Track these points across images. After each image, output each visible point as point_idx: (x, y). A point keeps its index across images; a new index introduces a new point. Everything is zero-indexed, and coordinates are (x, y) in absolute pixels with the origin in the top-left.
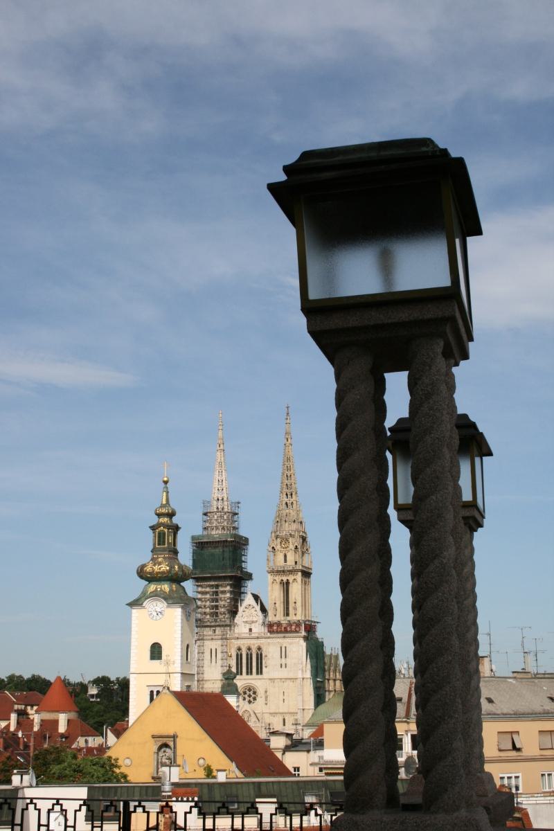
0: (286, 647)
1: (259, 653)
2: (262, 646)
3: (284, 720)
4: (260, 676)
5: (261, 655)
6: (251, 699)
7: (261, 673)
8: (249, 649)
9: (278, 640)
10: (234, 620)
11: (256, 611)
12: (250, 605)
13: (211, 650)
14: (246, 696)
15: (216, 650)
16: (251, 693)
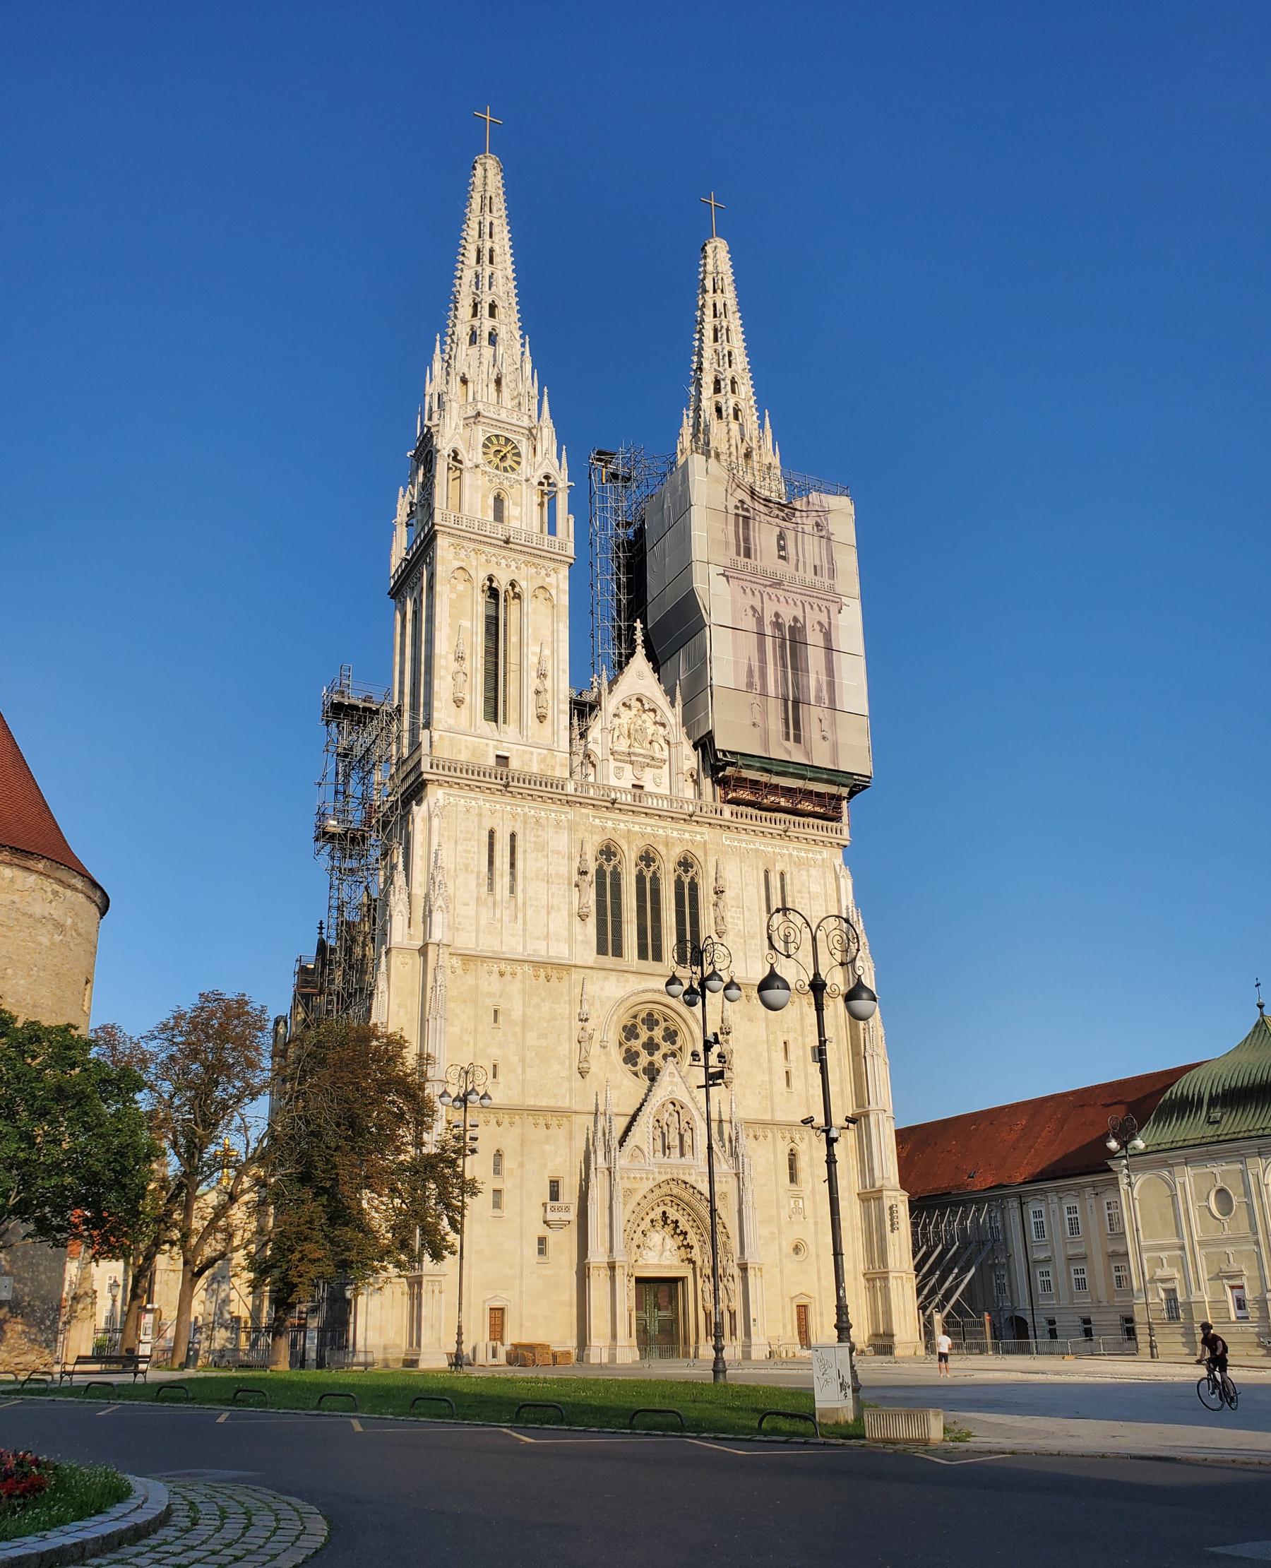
0: (782, 874)
1: (687, 881)
2: (699, 854)
3: (793, 1156)
5: (694, 887)
8: (647, 858)
9: (759, 844)
10: (583, 736)
13: (492, 834)
15: (513, 836)
16: (658, 1033)
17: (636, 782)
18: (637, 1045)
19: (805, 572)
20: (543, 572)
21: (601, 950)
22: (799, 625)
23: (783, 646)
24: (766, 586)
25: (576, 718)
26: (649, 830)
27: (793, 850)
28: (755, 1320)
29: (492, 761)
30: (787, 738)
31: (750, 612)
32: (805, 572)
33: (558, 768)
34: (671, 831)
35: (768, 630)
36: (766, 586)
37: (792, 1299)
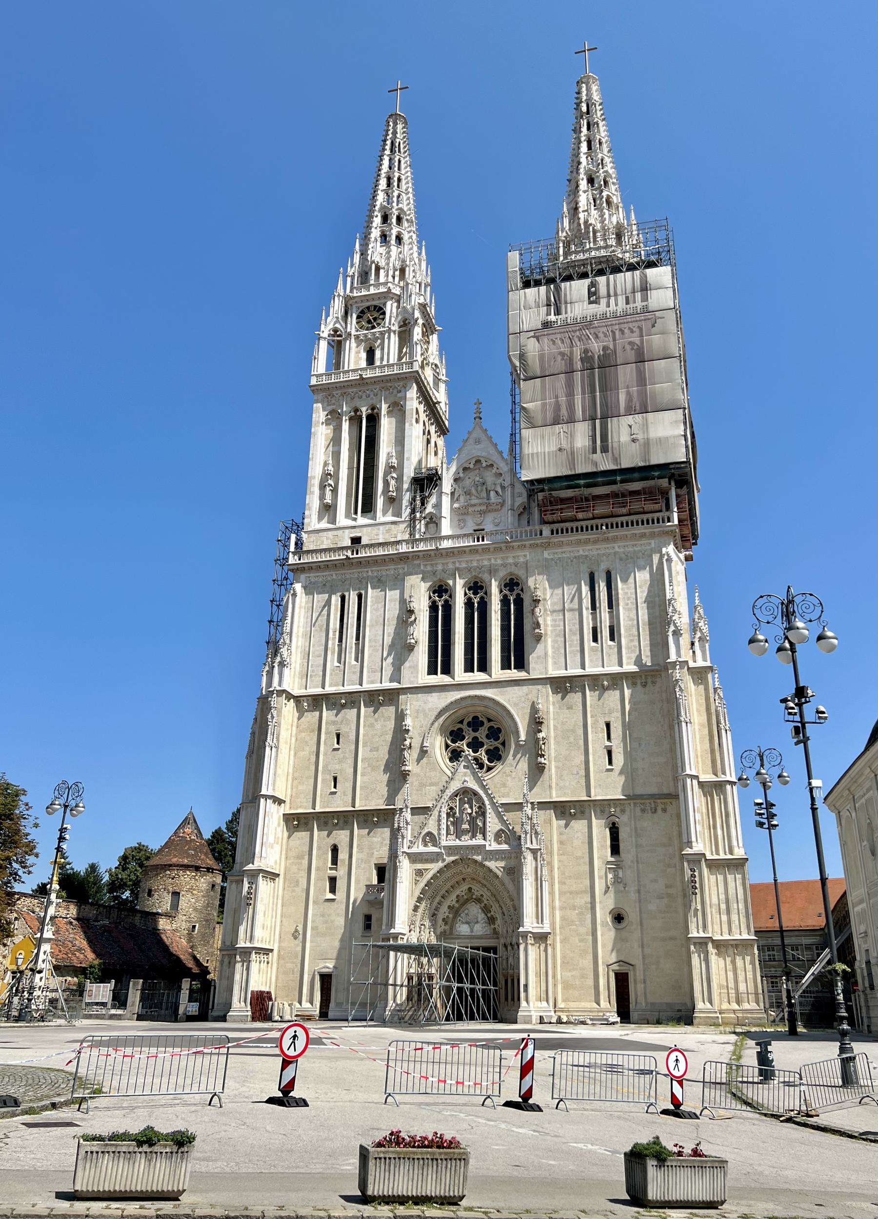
4: (514, 674)
5: (519, 602)
6: (482, 754)
7: (521, 665)
9: (582, 551)
11: (501, 474)
12: (478, 462)
14: (463, 745)
16: (482, 734)
17: (476, 528)
18: (463, 745)
19: (617, 305)
20: (395, 391)
21: (432, 670)
22: (609, 351)
23: (592, 377)
24: (574, 331)
25: (418, 491)
26: (475, 564)
27: (617, 547)
28: (526, 986)
29: (348, 543)
30: (594, 451)
31: (559, 358)
32: (617, 305)
33: (399, 535)
34: (496, 560)
35: (578, 365)
36: (574, 331)
37: (608, 966)
